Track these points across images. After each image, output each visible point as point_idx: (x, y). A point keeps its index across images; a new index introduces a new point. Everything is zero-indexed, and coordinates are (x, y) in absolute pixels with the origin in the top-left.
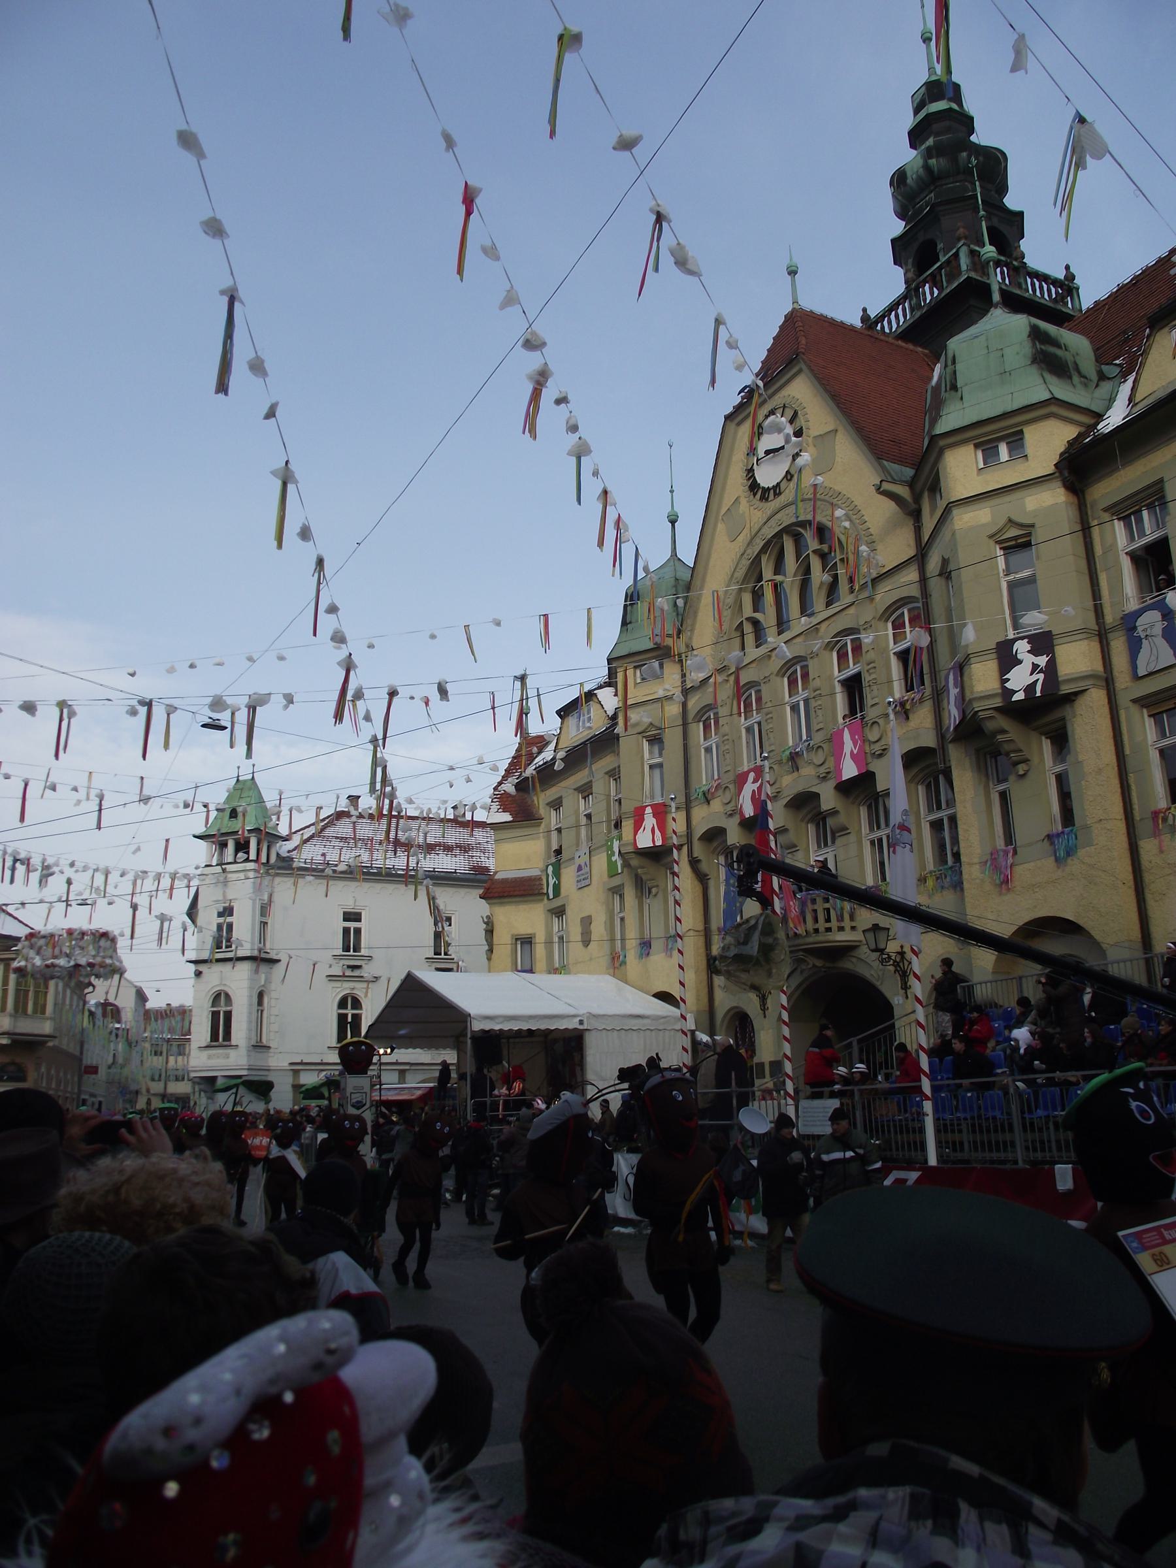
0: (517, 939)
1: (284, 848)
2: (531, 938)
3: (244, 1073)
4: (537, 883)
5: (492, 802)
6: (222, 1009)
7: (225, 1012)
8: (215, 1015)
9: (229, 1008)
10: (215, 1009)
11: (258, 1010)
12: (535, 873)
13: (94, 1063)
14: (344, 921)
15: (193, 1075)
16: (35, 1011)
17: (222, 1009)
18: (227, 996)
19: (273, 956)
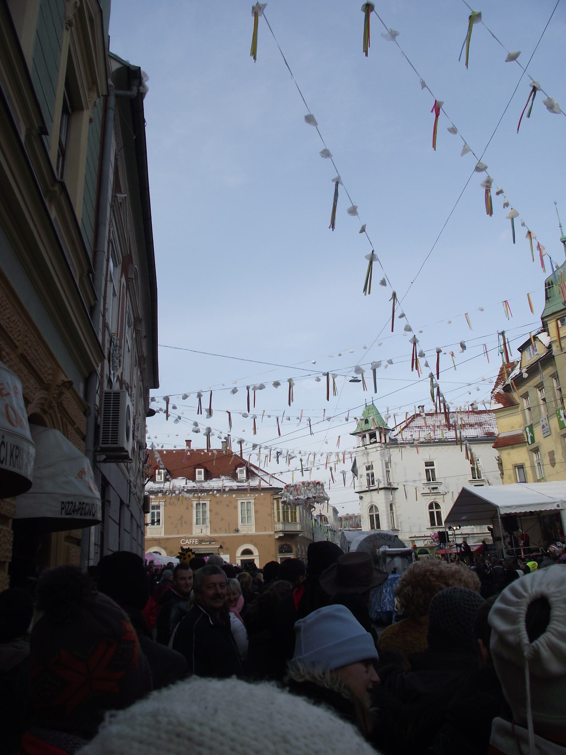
1: (392, 435)
2: (523, 465)
4: (522, 437)
5: (491, 399)
6: (374, 514)
7: (376, 515)
8: (371, 517)
9: (377, 513)
10: (371, 514)
11: (391, 513)
12: (519, 431)
14: (426, 466)
16: (292, 521)
17: (374, 514)
18: (376, 507)
19: (395, 486)
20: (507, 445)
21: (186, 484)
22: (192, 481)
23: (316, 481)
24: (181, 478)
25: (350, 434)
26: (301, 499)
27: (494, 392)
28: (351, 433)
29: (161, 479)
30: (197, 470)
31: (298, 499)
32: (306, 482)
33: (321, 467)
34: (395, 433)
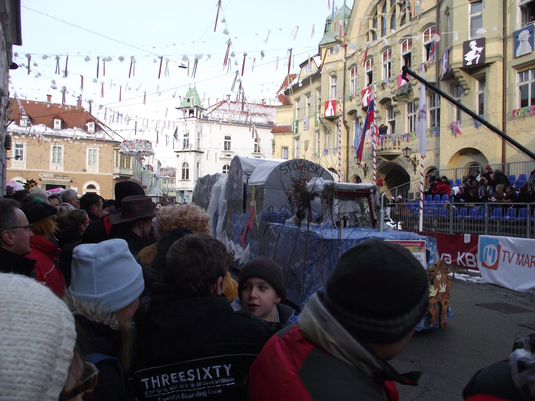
0: (283, 148)
1: (205, 113)
6: (186, 168)
7: (187, 169)
8: (183, 170)
9: (188, 168)
13: (146, 185)
15: (177, 190)
16: (127, 167)
17: (186, 168)
18: (187, 163)
20: (280, 132)
21: (46, 130)
22: (50, 128)
23: (147, 140)
24: (42, 125)
25: (176, 108)
28: (177, 107)
29: (25, 124)
30: (55, 120)
31: (132, 151)
34: (207, 112)
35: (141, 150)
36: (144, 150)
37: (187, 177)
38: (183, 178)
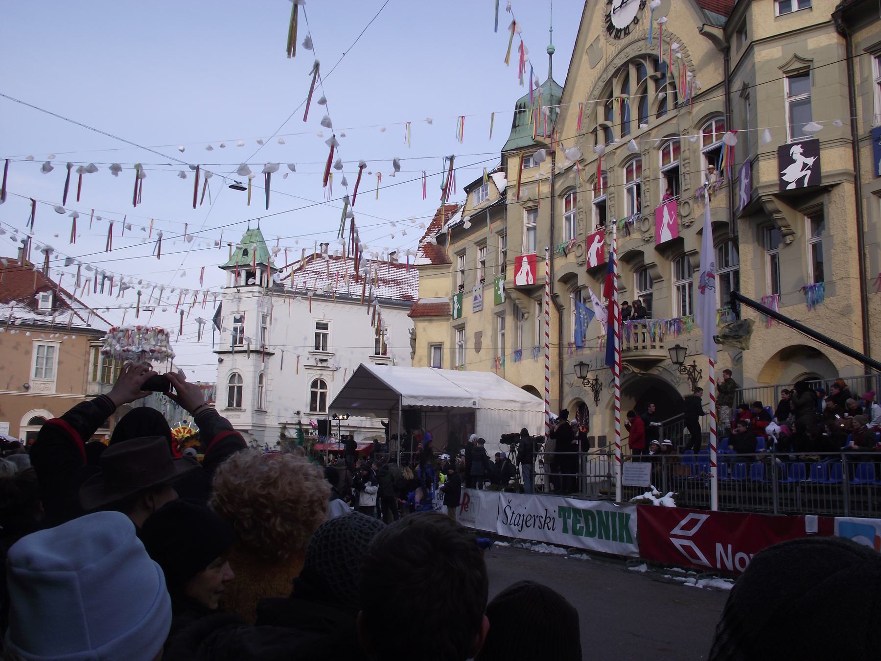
1: (277, 277)
3: (250, 428)
6: (236, 385)
8: (231, 389)
9: (240, 385)
12: (446, 300)
18: (239, 376)
19: (271, 350)
20: (427, 316)
23: (159, 328)
25: (220, 267)
26: (133, 352)
27: (423, 241)
28: (221, 266)
31: (128, 350)
32: (143, 327)
33: (168, 308)
34: (283, 275)
35: (147, 348)
36: (152, 348)
37: (239, 404)
38: (230, 404)
